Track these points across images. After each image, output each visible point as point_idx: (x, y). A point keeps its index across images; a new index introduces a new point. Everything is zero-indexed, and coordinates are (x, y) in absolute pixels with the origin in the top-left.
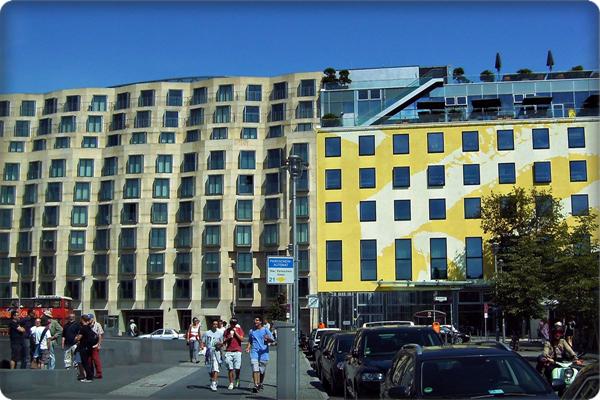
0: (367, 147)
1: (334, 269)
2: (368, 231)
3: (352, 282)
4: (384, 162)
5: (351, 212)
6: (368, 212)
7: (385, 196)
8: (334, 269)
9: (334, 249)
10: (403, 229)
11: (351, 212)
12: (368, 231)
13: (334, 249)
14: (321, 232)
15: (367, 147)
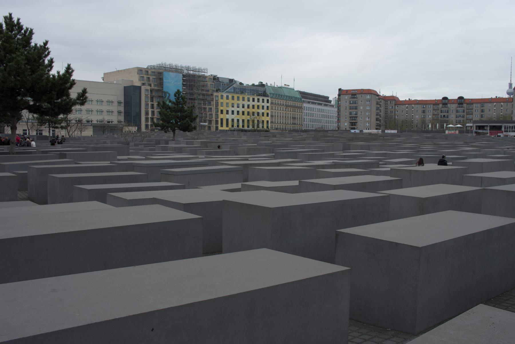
0: (227, 98)
1: (222, 124)
2: (228, 116)
3: (225, 128)
4: (230, 101)
5: (225, 112)
6: (227, 112)
7: (230, 109)
8: (222, 126)
9: (222, 120)
10: (233, 117)
11: (225, 112)
12: (228, 116)
13: (222, 120)
14: (221, 116)
15: (227, 98)
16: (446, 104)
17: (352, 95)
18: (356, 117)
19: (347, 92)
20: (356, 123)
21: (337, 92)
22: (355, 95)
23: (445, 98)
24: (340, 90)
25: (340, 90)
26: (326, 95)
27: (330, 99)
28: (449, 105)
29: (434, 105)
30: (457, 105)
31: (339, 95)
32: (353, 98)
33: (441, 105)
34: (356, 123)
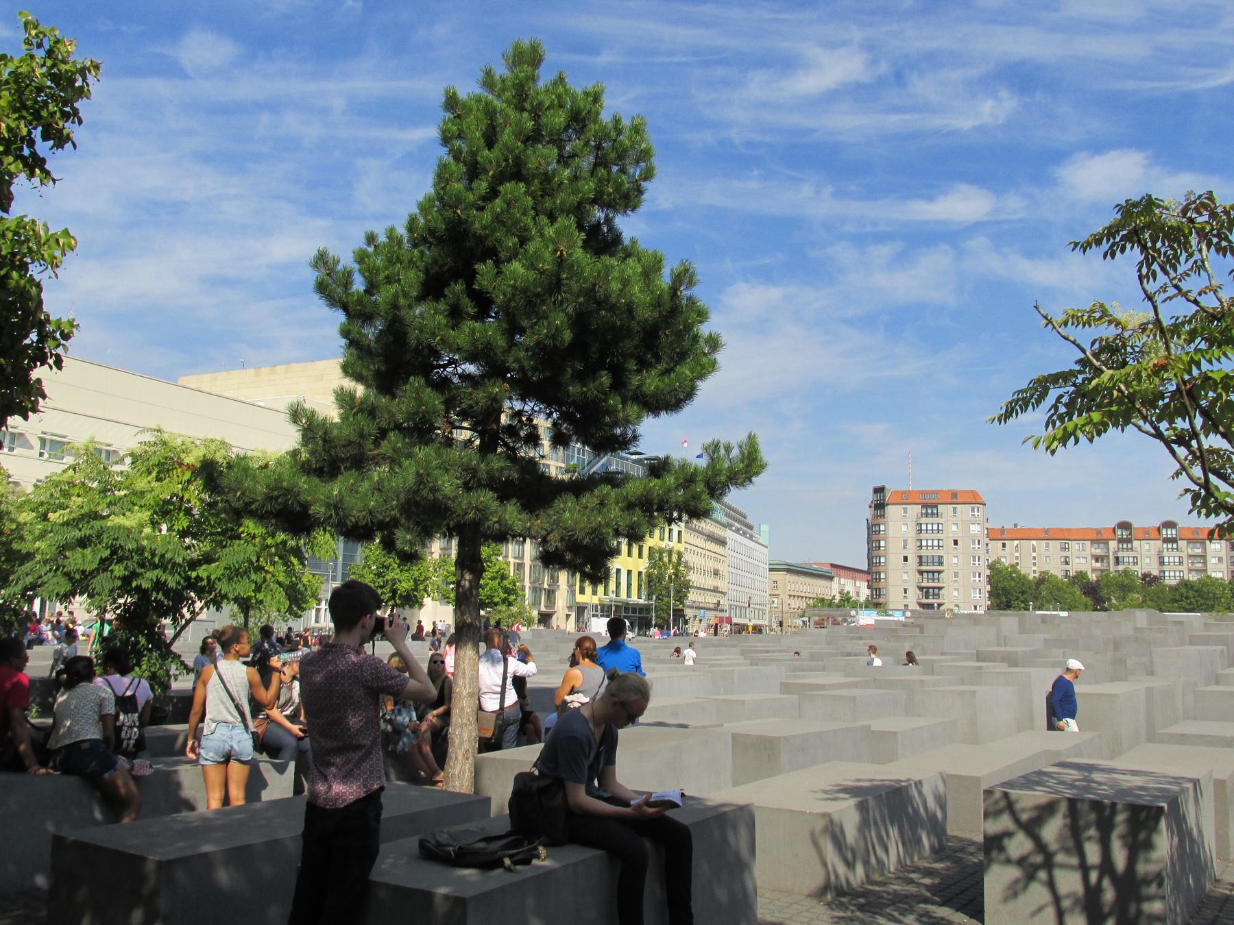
16: (1129, 541)
17: (925, 506)
18: (939, 572)
19: (905, 499)
20: (940, 588)
21: (870, 497)
22: (935, 506)
23: (1125, 526)
24: (879, 490)
25: (879, 490)
26: (743, 511)
27: (748, 520)
28: (1136, 543)
29: (1093, 541)
30: (1160, 542)
31: (880, 506)
32: (927, 514)
33: (1113, 545)
34: (940, 588)
